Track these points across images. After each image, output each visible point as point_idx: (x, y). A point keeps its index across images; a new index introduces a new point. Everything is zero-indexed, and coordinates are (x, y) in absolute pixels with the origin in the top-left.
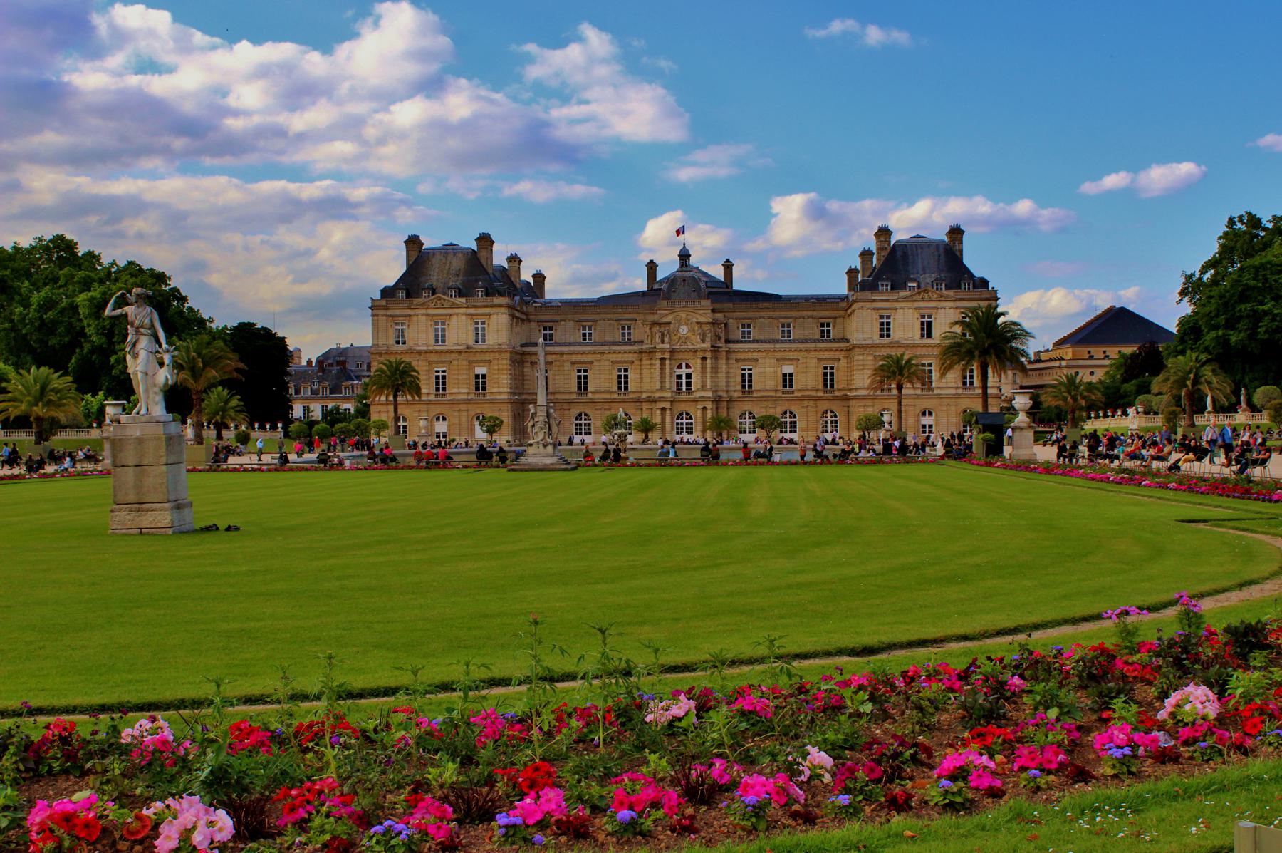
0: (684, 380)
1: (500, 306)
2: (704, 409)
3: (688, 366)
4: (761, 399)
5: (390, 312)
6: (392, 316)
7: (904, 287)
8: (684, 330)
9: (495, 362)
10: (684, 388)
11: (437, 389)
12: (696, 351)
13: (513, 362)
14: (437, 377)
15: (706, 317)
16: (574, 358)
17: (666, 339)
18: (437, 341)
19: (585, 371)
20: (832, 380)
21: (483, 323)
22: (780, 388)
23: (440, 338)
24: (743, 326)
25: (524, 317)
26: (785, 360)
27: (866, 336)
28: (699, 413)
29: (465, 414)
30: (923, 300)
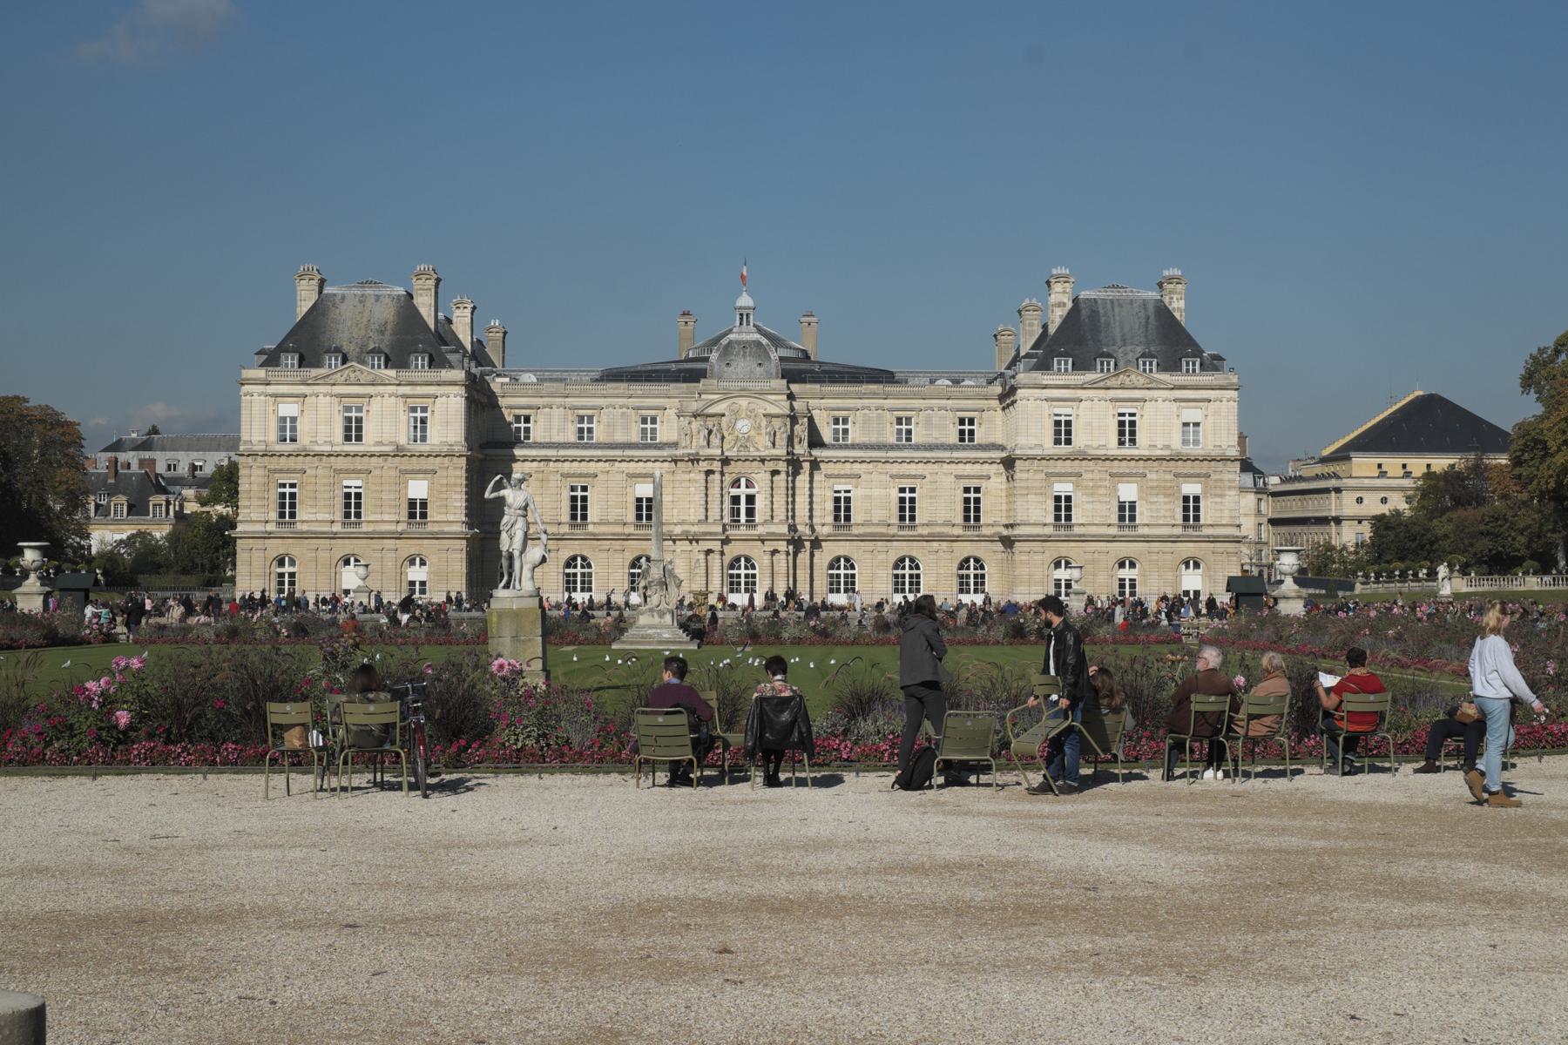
0: (743, 506)
2: (774, 552)
3: (749, 485)
4: (862, 538)
5: (271, 389)
6: (275, 396)
8: (743, 426)
10: (743, 518)
11: (347, 515)
12: (763, 461)
14: (348, 496)
17: (715, 440)
18: (348, 438)
19: (584, 489)
20: (977, 510)
21: (424, 409)
22: (895, 520)
23: (353, 430)
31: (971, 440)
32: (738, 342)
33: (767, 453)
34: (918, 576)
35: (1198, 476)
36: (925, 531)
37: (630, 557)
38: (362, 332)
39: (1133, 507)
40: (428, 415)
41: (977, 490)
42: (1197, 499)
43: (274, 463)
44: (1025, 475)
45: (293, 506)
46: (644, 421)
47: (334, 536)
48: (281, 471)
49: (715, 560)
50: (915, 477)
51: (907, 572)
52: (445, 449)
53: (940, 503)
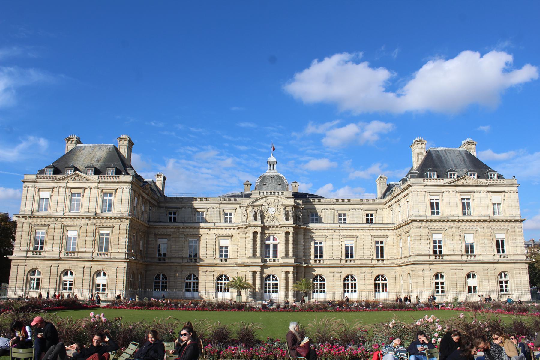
0: (271, 250)
1: (125, 182)
5: (38, 185)
6: (39, 188)
7: (447, 177)
8: (272, 211)
9: (117, 227)
10: (271, 256)
13: (132, 227)
15: (291, 202)
16: (187, 231)
17: (258, 217)
20: (382, 252)
21: (111, 195)
22: (344, 257)
24: (312, 215)
25: (156, 204)
26: (347, 237)
27: (422, 212)
28: (283, 276)
29: (87, 270)
30: (463, 186)
31: (372, 223)
32: (269, 176)
33: (283, 223)
34: (355, 284)
35: (503, 229)
36: (359, 262)
37: (216, 275)
38: (89, 161)
39: (472, 247)
40: (112, 198)
41: (382, 243)
42: (502, 241)
43: (34, 221)
44: (418, 230)
45: (42, 243)
46: (226, 214)
47: (60, 259)
48: (38, 225)
49: (258, 276)
50: (353, 237)
51: (350, 282)
52: (119, 215)
53: (364, 250)
